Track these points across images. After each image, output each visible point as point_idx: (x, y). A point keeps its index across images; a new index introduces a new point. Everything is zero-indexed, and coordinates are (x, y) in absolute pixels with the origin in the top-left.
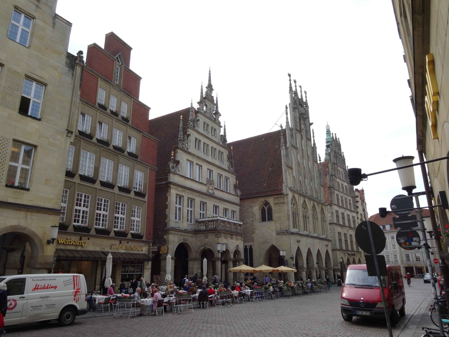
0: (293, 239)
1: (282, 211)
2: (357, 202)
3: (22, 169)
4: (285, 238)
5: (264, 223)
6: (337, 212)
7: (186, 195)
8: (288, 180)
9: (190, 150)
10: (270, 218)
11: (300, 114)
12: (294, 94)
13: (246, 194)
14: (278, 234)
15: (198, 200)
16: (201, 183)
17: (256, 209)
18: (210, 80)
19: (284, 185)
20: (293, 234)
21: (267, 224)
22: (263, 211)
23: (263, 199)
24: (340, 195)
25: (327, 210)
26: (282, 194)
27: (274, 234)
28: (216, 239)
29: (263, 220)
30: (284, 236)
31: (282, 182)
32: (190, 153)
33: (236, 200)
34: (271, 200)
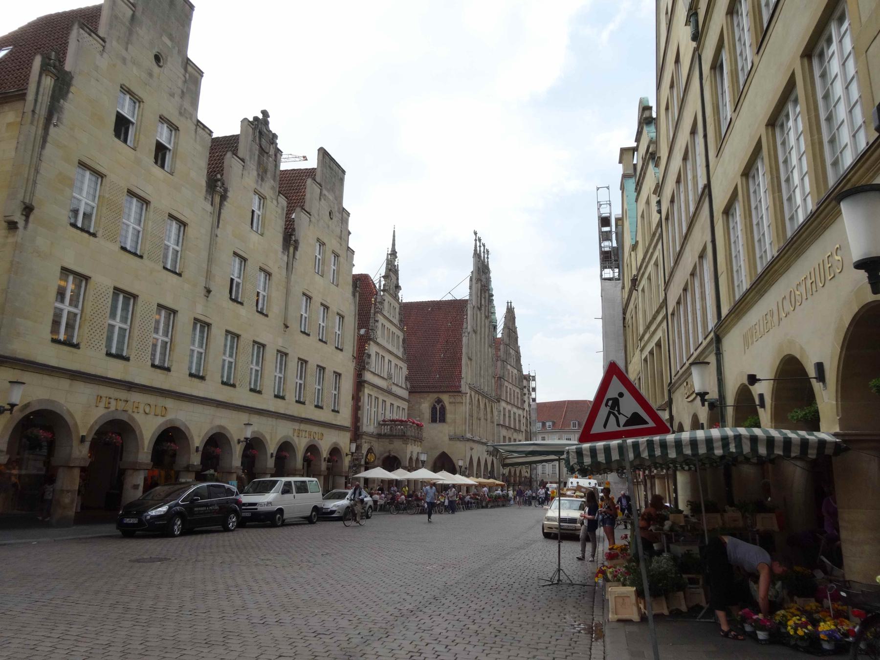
0: (469, 444)
1: (458, 412)
2: (525, 394)
3: (120, 328)
4: (460, 445)
5: (434, 425)
6: (504, 409)
7: (374, 394)
8: (468, 374)
9: (378, 340)
10: (443, 420)
11: (482, 286)
12: (477, 255)
13: (416, 389)
14: (451, 439)
15: (381, 398)
16: (383, 378)
17: (425, 406)
18: (394, 245)
19: (463, 382)
20: (468, 440)
21: (438, 426)
22: (434, 409)
23: (435, 396)
24: (510, 386)
25: (495, 406)
26: (460, 392)
27: (447, 438)
28: (404, 446)
29: (434, 420)
30: (458, 442)
31: (460, 378)
32: (378, 344)
33: (404, 394)
34: (445, 398)
